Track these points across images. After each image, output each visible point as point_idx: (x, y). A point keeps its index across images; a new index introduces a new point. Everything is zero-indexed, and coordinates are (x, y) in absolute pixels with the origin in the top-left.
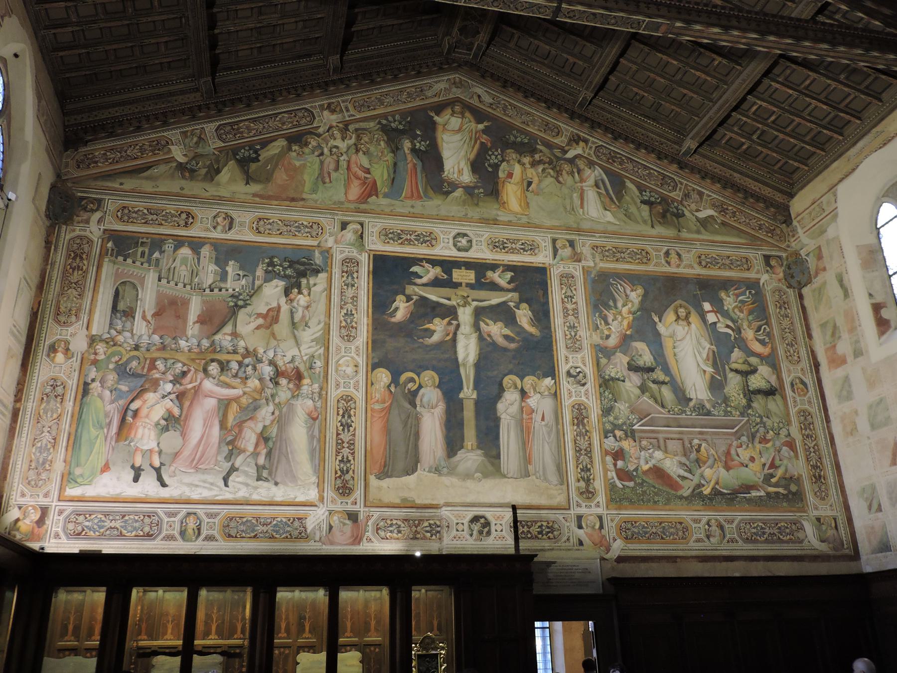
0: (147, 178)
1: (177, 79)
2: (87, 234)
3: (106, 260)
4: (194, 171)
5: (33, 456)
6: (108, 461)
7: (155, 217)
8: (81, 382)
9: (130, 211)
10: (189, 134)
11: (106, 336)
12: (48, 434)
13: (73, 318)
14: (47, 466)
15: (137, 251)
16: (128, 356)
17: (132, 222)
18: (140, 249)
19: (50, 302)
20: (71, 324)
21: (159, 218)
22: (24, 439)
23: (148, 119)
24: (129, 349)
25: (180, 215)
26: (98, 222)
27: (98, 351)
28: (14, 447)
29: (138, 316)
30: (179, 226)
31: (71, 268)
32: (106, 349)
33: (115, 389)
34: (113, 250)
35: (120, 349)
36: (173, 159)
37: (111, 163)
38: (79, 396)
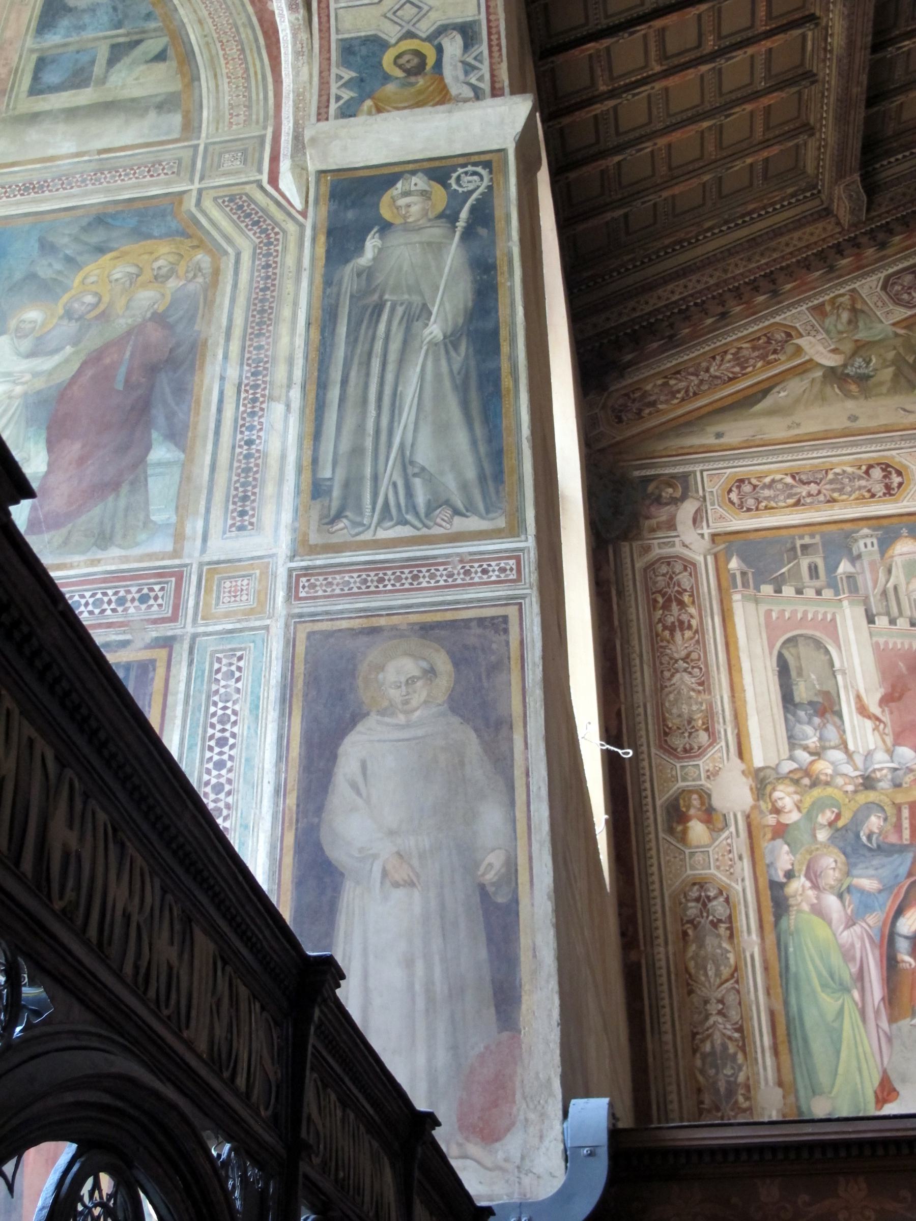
0: (771, 412)
1: (783, 199)
2: (678, 549)
3: (737, 597)
4: (868, 377)
5: (701, 1078)
6: (885, 1072)
7: (813, 488)
8: (763, 883)
9: (755, 487)
10: (828, 308)
11: (787, 767)
12: (720, 1019)
13: (703, 737)
14: (741, 1099)
15: (798, 564)
16: (854, 806)
17: (766, 508)
18: (804, 563)
19: (641, 710)
20: (702, 751)
21: (826, 488)
22: (668, 1038)
23: (737, 293)
24: (850, 788)
25: (867, 472)
26: (695, 521)
27: (780, 804)
28: (651, 1060)
29: (847, 707)
30: (873, 496)
31: (665, 628)
32: (797, 797)
33: (848, 889)
34: (744, 574)
35: (829, 790)
36: (809, 366)
37: (683, 400)
38: (769, 918)
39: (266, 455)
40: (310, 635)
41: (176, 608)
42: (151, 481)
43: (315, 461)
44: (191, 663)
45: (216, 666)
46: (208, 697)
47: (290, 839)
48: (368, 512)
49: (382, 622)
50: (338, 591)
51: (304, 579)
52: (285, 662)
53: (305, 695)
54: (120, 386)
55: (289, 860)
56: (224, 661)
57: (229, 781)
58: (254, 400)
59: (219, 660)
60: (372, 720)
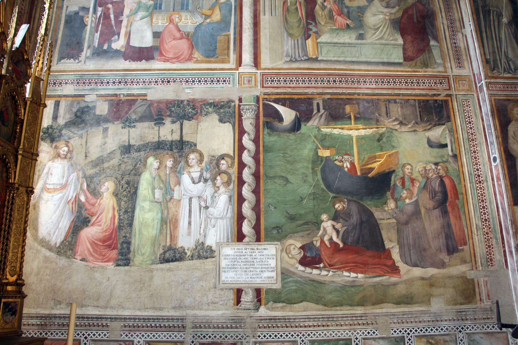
39: (460, 48)
40: (495, 100)
41: (449, 86)
42: (433, 50)
43: (485, 54)
44: (457, 101)
45: (463, 103)
46: (464, 111)
47: (502, 149)
48: (501, 69)
49: (510, 98)
50: (498, 89)
51: (490, 85)
52: (491, 106)
53: (497, 114)
54: (415, 21)
55: (503, 154)
56: (465, 102)
57: (474, 133)
58: (453, 31)
59: (464, 102)
60: (513, 122)
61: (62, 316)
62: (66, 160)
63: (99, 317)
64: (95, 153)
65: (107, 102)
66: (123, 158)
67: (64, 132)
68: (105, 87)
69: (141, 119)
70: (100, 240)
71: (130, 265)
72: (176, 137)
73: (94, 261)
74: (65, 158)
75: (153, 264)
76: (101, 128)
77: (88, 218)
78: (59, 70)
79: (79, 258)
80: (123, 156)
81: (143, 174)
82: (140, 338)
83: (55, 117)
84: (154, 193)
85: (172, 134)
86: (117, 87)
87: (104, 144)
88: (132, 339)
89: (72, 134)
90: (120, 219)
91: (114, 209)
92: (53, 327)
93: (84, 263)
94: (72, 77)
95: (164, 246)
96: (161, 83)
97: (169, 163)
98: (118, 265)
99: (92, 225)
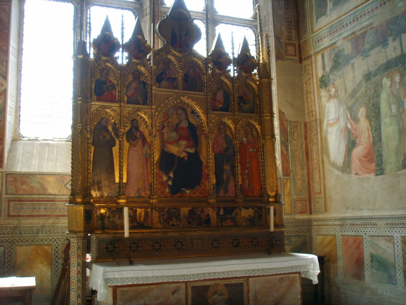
61: (351, 218)
62: (335, 99)
63: (371, 217)
64: (350, 88)
65: (350, 42)
66: (367, 85)
67: (330, 77)
68: (346, 29)
69: (372, 48)
70: (363, 157)
71: (384, 173)
72: (398, 53)
73: (362, 174)
74: (335, 97)
75: (398, 170)
76: (350, 66)
77: (354, 140)
78: (318, 29)
79: (354, 173)
80: (367, 83)
81: (381, 95)
82: (398, 234)
83: (324, 68)
84: (390, 108)
85: (395, 51)
86: (353, 25)
87: (354, 78)
88: (392, 234)
89: (335, 77)
90: (373, 137)
91: (368, 129)
92: (347, 227)
93: (356, 176)
94: (326, 31)
95: (403, 154)
96: (379, 7)
97: (397, 79)
98: (377, 175)
99: (358, 146)
